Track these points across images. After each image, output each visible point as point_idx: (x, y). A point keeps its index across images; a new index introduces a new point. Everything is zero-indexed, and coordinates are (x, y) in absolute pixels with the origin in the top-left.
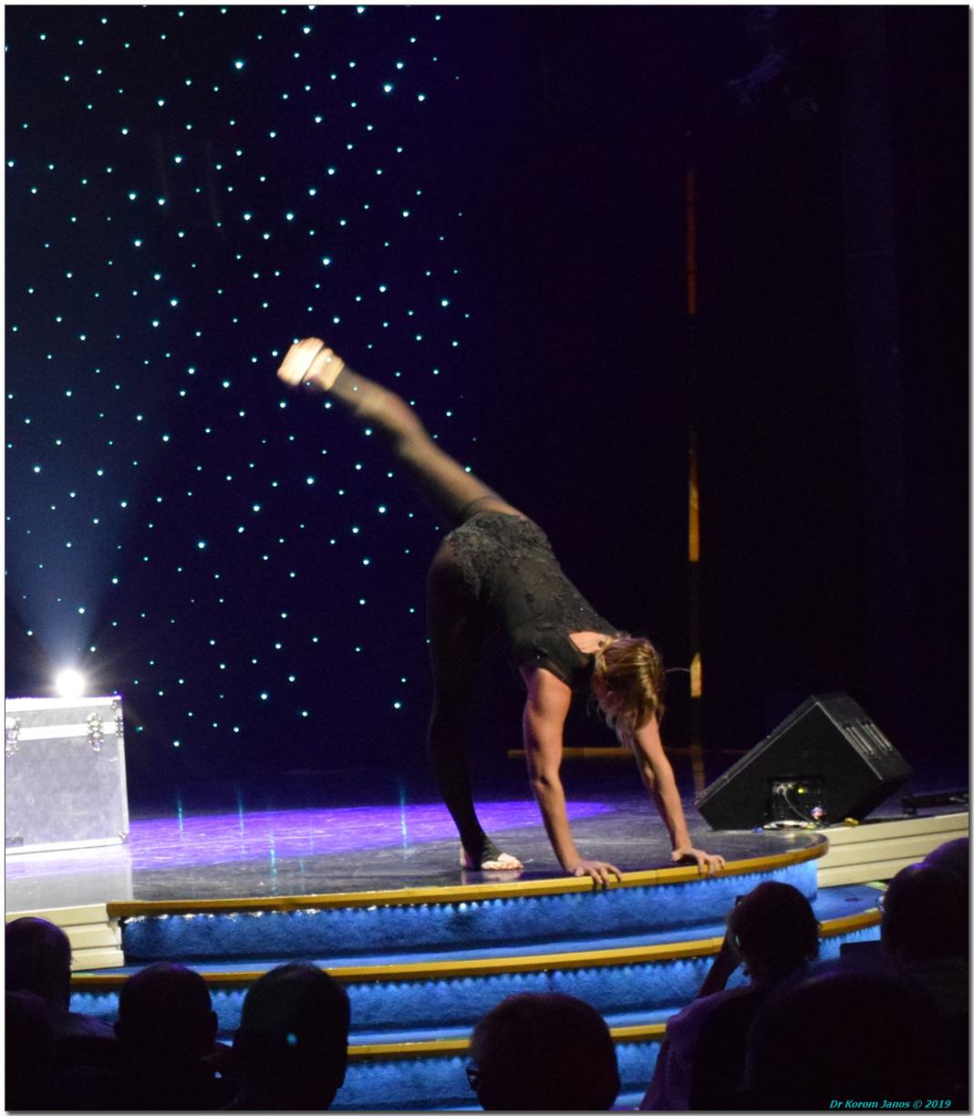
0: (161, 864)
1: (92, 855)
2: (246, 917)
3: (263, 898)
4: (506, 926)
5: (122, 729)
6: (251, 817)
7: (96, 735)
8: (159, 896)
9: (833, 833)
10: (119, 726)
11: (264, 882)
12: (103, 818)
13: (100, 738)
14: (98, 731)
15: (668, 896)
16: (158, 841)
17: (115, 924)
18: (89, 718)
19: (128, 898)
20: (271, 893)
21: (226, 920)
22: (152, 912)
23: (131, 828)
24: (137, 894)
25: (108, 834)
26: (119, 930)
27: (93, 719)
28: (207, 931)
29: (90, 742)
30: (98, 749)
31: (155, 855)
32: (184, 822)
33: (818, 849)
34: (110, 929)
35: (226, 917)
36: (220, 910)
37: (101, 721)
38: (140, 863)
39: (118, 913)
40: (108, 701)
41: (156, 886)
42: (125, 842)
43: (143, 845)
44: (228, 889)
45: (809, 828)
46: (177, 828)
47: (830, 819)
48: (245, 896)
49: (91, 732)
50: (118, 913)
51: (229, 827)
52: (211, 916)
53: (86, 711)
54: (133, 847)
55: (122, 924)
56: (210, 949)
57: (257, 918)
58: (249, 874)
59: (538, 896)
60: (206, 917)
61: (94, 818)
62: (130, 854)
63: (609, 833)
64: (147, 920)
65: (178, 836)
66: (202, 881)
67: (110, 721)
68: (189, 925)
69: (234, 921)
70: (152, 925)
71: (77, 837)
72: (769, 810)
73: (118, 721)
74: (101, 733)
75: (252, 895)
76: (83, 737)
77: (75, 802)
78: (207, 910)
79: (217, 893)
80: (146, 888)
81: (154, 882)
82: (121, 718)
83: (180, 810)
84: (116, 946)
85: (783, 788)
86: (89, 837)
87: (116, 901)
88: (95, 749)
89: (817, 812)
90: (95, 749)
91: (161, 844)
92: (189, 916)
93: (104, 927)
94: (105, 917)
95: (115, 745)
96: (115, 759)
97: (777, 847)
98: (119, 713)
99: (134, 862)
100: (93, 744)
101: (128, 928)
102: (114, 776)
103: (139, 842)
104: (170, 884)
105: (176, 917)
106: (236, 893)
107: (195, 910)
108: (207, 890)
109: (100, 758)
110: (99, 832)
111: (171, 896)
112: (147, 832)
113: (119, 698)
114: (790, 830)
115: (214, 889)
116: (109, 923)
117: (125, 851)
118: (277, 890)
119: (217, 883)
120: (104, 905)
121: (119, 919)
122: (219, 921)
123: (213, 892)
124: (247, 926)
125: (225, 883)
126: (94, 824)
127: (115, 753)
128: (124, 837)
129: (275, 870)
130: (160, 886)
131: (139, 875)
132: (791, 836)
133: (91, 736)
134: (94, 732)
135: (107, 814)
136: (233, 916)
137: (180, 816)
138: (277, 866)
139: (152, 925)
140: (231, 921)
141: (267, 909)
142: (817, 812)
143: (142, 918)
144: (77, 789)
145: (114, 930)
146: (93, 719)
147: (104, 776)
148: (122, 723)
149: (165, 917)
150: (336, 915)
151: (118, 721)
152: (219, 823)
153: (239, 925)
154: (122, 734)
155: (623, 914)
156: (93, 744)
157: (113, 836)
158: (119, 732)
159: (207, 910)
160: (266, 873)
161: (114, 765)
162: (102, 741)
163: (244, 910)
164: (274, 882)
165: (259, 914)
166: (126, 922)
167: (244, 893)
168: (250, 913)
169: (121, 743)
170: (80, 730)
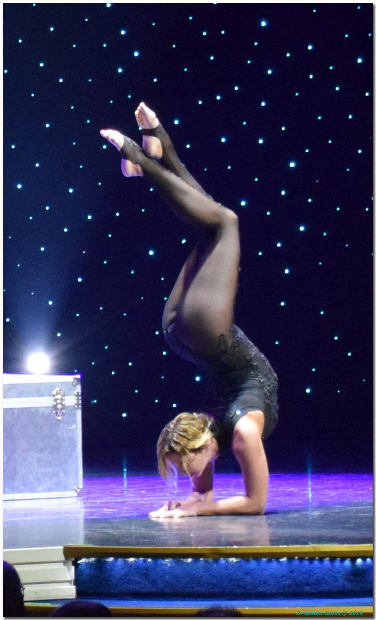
0: (109, 515)
1: (53, 505)
5: (80, 402)
7: (59, 406)
8: (106, 541)
10: (78, 399)
12: (62, 474)
13: (62, 409)
14: (61, 403)
16: (107, 496)
17: (71, 563)
18: (54, 392)
19: (81, 543)
22: (101, 555)
23: (85, 484)
24: (88, 539)
25: (66, 488)
26: (73, 568)
27: (57, 394)
28: (144, 572)
29: (54, 412)
30: (60, 418)
31: (103, 507)
32: (128, 480)
34: (66, 567)
35: (162, 562)
36: (158, 556)
37: (64, 395)
38: (92, 513)
40: (70, 379)
41: (103, 533)
42: (79, 495)
43: (94, 499)
46: (122, 484)
49: (55, 403)
50: (72, 554)
52: (150, 560)
53: (52, 386)
54: (85, 500)
55: (75, 564)
60: (145, 561)
61: (56, 474)
62: (83, 505)
64: (96, 561)
65: (123, 492)
67: (69, 395)
69: (169, 565)
70: (100, 565)
71: (41, 489)
73: (78, 395)
74: (64, 405)
76: (47, 407)
77: (39, 460)
78: (146, 555)
79: (155, 541)
80: (96, 535)
81: (106, 531)
82: (80, 393)
83: (125, 470)
84: (70, 582)
86: (50, 490)
87: (71, 544)
88: (58, 418)
90: (58, 418)
91: (109, 498)
92: (131, 560)
93: (61, 566)
94: (62, 557)
95: (74, 415)
96: (74, 426)
98: (79, 389)
99: (85, 512)
100: (57, 413)
101: (80, 567)
102: (73, 441)
103: (91, 496)
104: (115, 532)
105: (120, 560)
108: (147, 539)
109: (61, 426)
110: (60, 486)
112: (98, 487)
113: (79, 376)
115: (153, 537)
116: (65, 563)
117: (79, 503)
120: (61, 547)
121: (73, 559)
122: (157, 564)
126: (55, 480)
127: (75, 422)
128: (79, 490)
130: (107, 533)
131: (89, 522)
133: (55, 407)
134: (57, 404)
135: (66, 472)
136: (168, 561)
137: (125, 474)
139: (100, 565)
140: (166, 565)
143: (92, 559)
144: (42, 450)
145: (69, 569)
146: (57, 394)
147: (64, 440)
148: (80, 397)
149: (111, 559)
151: (78, 395)
154: (80, 407)
156: (57, 413)
157: (70, 490)
158: (78, 404)
159: (146, 555)
161: (73, 432)
162: (64, 411)
166: (79, 562)
169: (79, 414)
170: (46, 402)
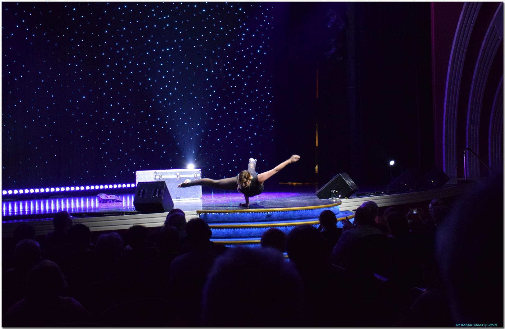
4: (277, 217)
9: (343, 200)
15: (310, 212)
28: (217, 217)
33: (340, 203)
36: (220, 212)
45: (338, 199)
47: (342, 198)
56: (217, 220)
59: (284, 211)
63: (299, 199)
72: (330, 195)
78: (217, 212)
85: (333, 191)
89: (340, 196)
97: (332, 203)
107: (215, 212)
114: (335, 200)
124: (225, 216)
132: (334, 201)
141: (229, 212)
142: (340, 196)
150: (243, 214)
152: (220, 195)
155: (301, 215)
159: (217, 212)
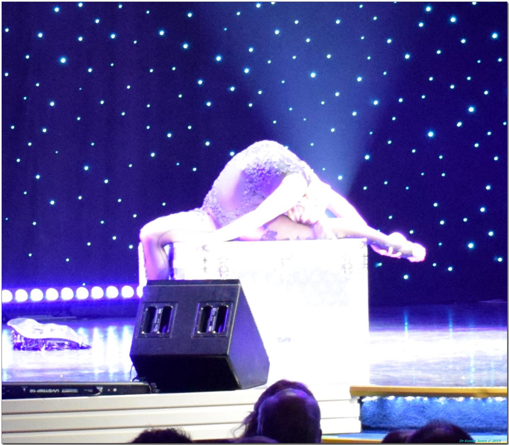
2: (449, 401)
3: (464, 388)
6: (458, 331)
8: (388, 383)
11: (466, 376)
20: (470, 385)
21: (436, 403)
22: (383, 394)
36: (432, 395)
39: (359, 394)
44: (440, 381)
48: (451, 385)
50: (359, 394)
51: (441, 337)
52: (426, 399)
57: (459, 402)
58: (454, 370)
60: (422, 400)
64: (379, 400)
66: (420, 374)
68: (409, 405)
69: (443, 403)
75: (457, 385)
80: (379, 377)
92: (409, 399)
105: (400, 399)
106: (444, 383)
107: (415, 394)
111: (397, 383)
115: (428, 380)
118: (475, 383)
119: (430, 376)
122: (431, 403)
123: (429, 381)
124: (452, 408)
125: (437, 376)
129: (473, 370)
136: (442, 400)
138: (475, 366)
140: (440, 403)
141: (467, 396)
143: (375, 398)
149: (391, 398)
153: (446, 406)
160: (466, 370)
163: (448, 395)
164: (472, 377)
165: (461, 399)
167: (451, 383)
168: (454, 398)
